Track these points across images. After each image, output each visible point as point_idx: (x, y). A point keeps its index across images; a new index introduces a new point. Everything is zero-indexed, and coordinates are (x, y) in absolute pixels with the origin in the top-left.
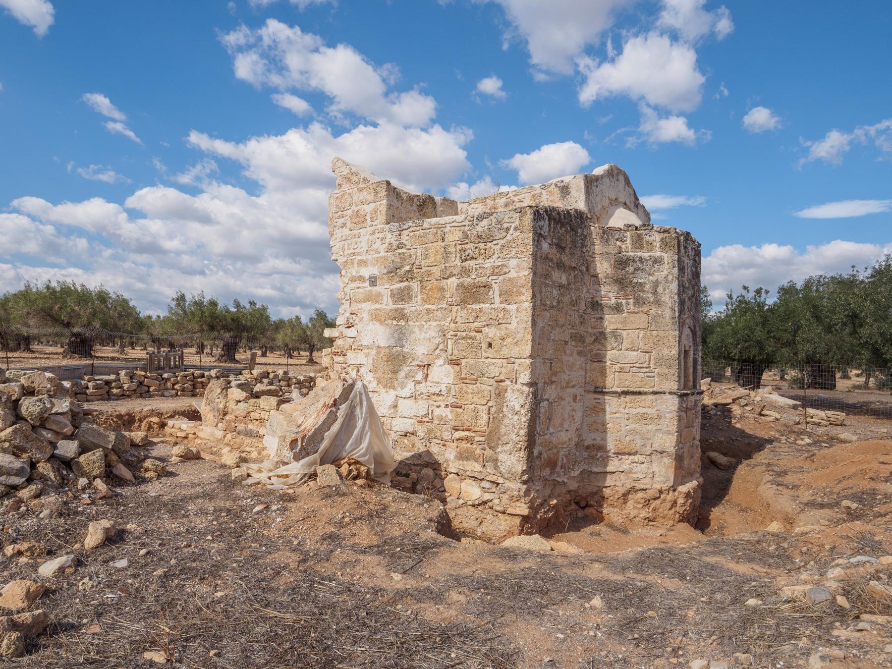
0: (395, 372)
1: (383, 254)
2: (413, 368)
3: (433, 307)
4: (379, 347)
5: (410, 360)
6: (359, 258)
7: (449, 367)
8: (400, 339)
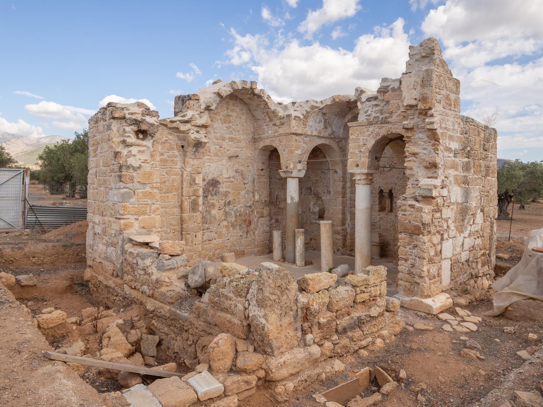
0: (463, 220)
3: (477, 177)
5: (469, 211)
6: (449, 133)
8: (467, 198)
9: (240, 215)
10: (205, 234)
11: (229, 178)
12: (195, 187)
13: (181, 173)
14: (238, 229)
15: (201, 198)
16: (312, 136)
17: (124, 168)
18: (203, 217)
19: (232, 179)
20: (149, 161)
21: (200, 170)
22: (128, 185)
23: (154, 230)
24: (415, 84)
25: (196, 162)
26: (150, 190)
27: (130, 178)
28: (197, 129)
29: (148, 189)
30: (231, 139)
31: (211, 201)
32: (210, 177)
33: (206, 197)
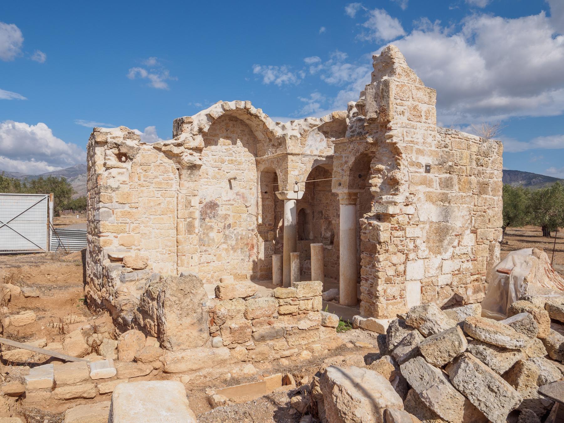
0: (441, 241)
1: (434, 148)
2: (453, 237)
3: (464, 194)
4: (432, 222)
5: (451, 232)
6: (417, 146)
7: (472, 234)
8: (446, 216)
9: (241, 238)
10: (203, 256)
11: (229, 200)
12: (191, 209)
13: (176, 195)
14: (240, 252)
15: (198, 220)
16: (311, 155)
17: (103, 189)
18: (200, 239)
19: (231, 202)
20: (127, 182)
21: (196, 192)
22: (106, 205)
23: (133, 247)
24: (376, 96)
25: (191, 184)
26: (129, 210)
27: (109, 198)
28: (191, 151)
29: (127, 208)
30: (231, 162)
31: (209, 224)
32: (208, 200)
33: (204, 219)
